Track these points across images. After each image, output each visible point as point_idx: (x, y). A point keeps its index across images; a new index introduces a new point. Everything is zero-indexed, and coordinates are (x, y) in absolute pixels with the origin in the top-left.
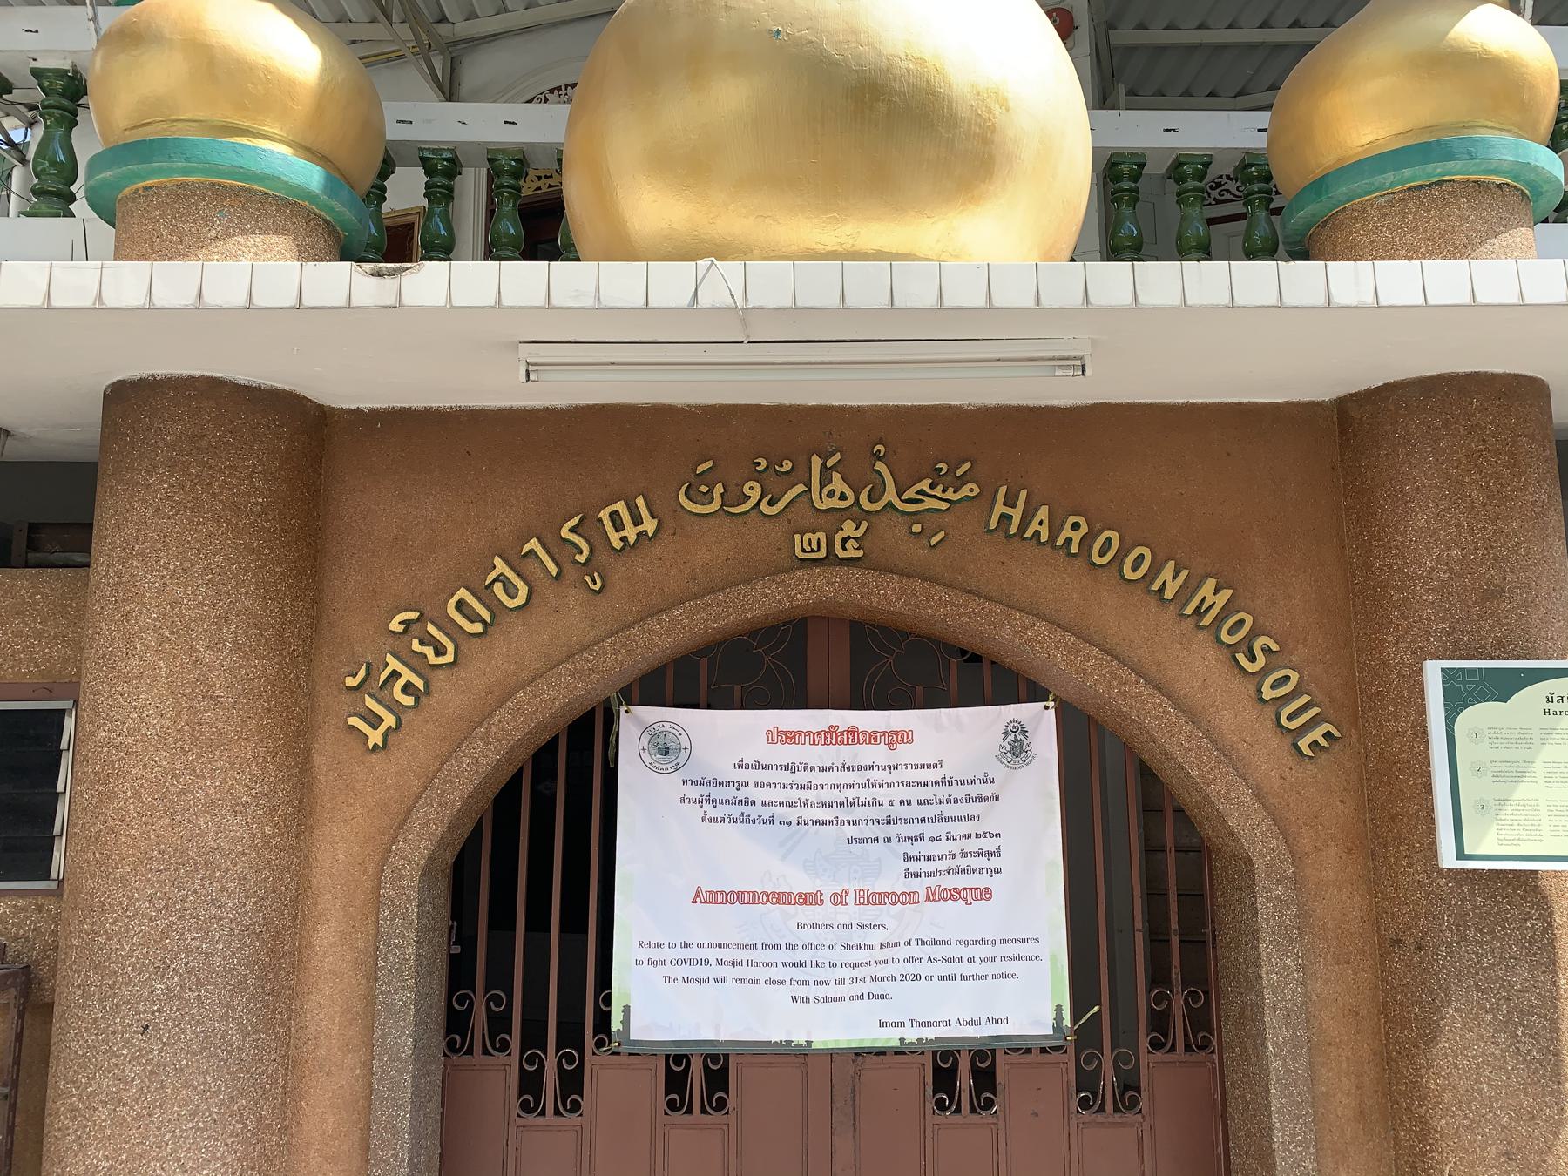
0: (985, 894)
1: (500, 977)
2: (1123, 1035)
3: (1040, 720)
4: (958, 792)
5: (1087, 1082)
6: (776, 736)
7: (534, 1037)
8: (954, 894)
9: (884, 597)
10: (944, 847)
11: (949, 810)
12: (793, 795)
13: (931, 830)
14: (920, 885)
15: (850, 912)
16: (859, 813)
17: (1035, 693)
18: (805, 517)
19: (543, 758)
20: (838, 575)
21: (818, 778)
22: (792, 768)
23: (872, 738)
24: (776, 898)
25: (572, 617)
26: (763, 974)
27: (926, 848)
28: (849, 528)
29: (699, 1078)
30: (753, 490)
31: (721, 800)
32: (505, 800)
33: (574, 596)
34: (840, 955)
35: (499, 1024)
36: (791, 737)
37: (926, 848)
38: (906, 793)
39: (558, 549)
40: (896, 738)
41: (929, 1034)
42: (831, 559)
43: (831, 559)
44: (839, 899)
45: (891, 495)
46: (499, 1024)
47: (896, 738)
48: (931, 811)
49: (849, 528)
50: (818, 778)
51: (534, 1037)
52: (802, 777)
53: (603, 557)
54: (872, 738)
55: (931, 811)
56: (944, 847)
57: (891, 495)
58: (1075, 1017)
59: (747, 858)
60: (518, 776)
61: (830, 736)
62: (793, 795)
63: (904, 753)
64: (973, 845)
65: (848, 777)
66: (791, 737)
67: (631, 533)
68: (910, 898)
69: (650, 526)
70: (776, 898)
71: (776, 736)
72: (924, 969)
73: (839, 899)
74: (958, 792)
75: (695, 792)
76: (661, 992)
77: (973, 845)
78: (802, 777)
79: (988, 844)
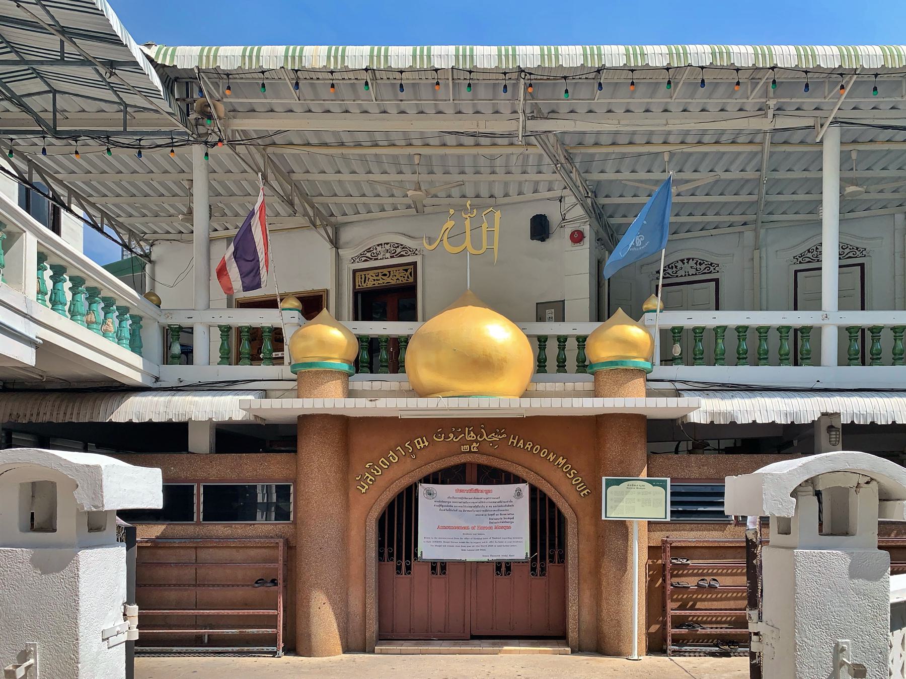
0: (509, 528)
1: (391, 544)
2: (543, 558)
3: (525, 488)
4: (504, 504)
5: (533, 569)
6: (457, 491)
7: (399, 557)
8: (502, 528)
9: (483, 460)
10: (499, 517)
11: (501, 508)
12: (462, 505)
13: (496, 513)
14: (493, 525)
15: (476, 531)
16: (478, 509)
17: (524, 481)
18: (464, 442)
19: (400, 496)
20: (472, 455)
21: (468, 501)
22: (462, 498)
23: (482, 491)
24: (458, 528)
25: (408, 464)
26: (455, 544)
27: (495, 517)
28: (475, 444)
29: (439, 567)
30: (451, 435)
31: (445, 506)
32: (391, 506)
33: (409, 460)
34: (473, 541)
35: (391, 555)
36: (461, 491)
37: (495, 517)
38: (489, 504)
39: (404, 448)
40: (488, 492)
41: (495, 558)
42: (470, 452)
43: (470, 452)
44: (473, 528)
45: (485, 437)
46: (391, 555)
47: (488, 492)
48: (496, 509)
49: (475, 444)
50: (468, 501)
51: (399, 557)
52: (464, 500)
53: (415, 450)
54: (482, 491)
55: (496, 509)
56: (499, 517)
57: (485, 437)
58: (531, 555)
59: (451, 519)
60: (394, 500)
61: (471, 491)
62: (462, 505)
63: (490, 495)
64: (507, 516)
65: (475, 501)
66: (461, 491)
67: (422, 445)
68: (491, 528)
69: (426, 444)
70: (458, 528)
71: (457, 491)
72: (494, 544)
73: (473, 528)
74: (504, 504)
75: (438, 504)
76: (429, 547)
77: (507, 516)
78: (464, 500)
79: (511, 516)
